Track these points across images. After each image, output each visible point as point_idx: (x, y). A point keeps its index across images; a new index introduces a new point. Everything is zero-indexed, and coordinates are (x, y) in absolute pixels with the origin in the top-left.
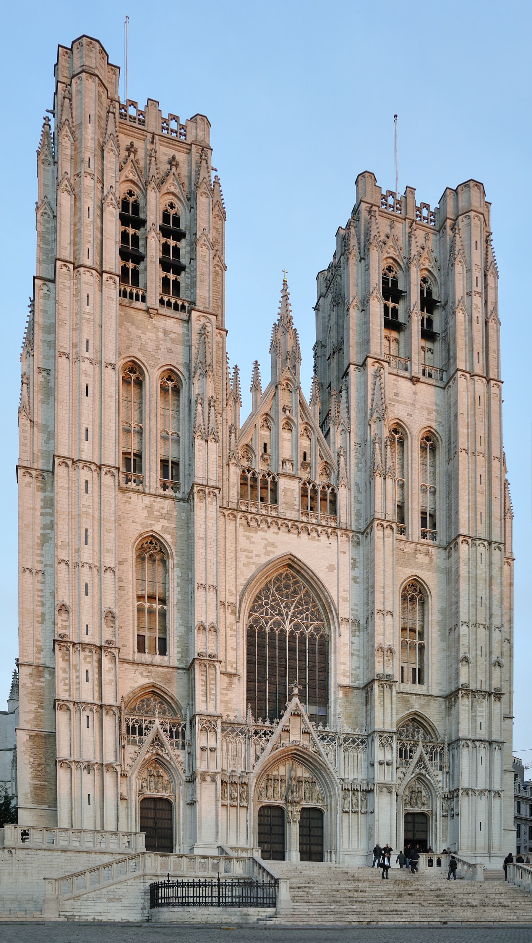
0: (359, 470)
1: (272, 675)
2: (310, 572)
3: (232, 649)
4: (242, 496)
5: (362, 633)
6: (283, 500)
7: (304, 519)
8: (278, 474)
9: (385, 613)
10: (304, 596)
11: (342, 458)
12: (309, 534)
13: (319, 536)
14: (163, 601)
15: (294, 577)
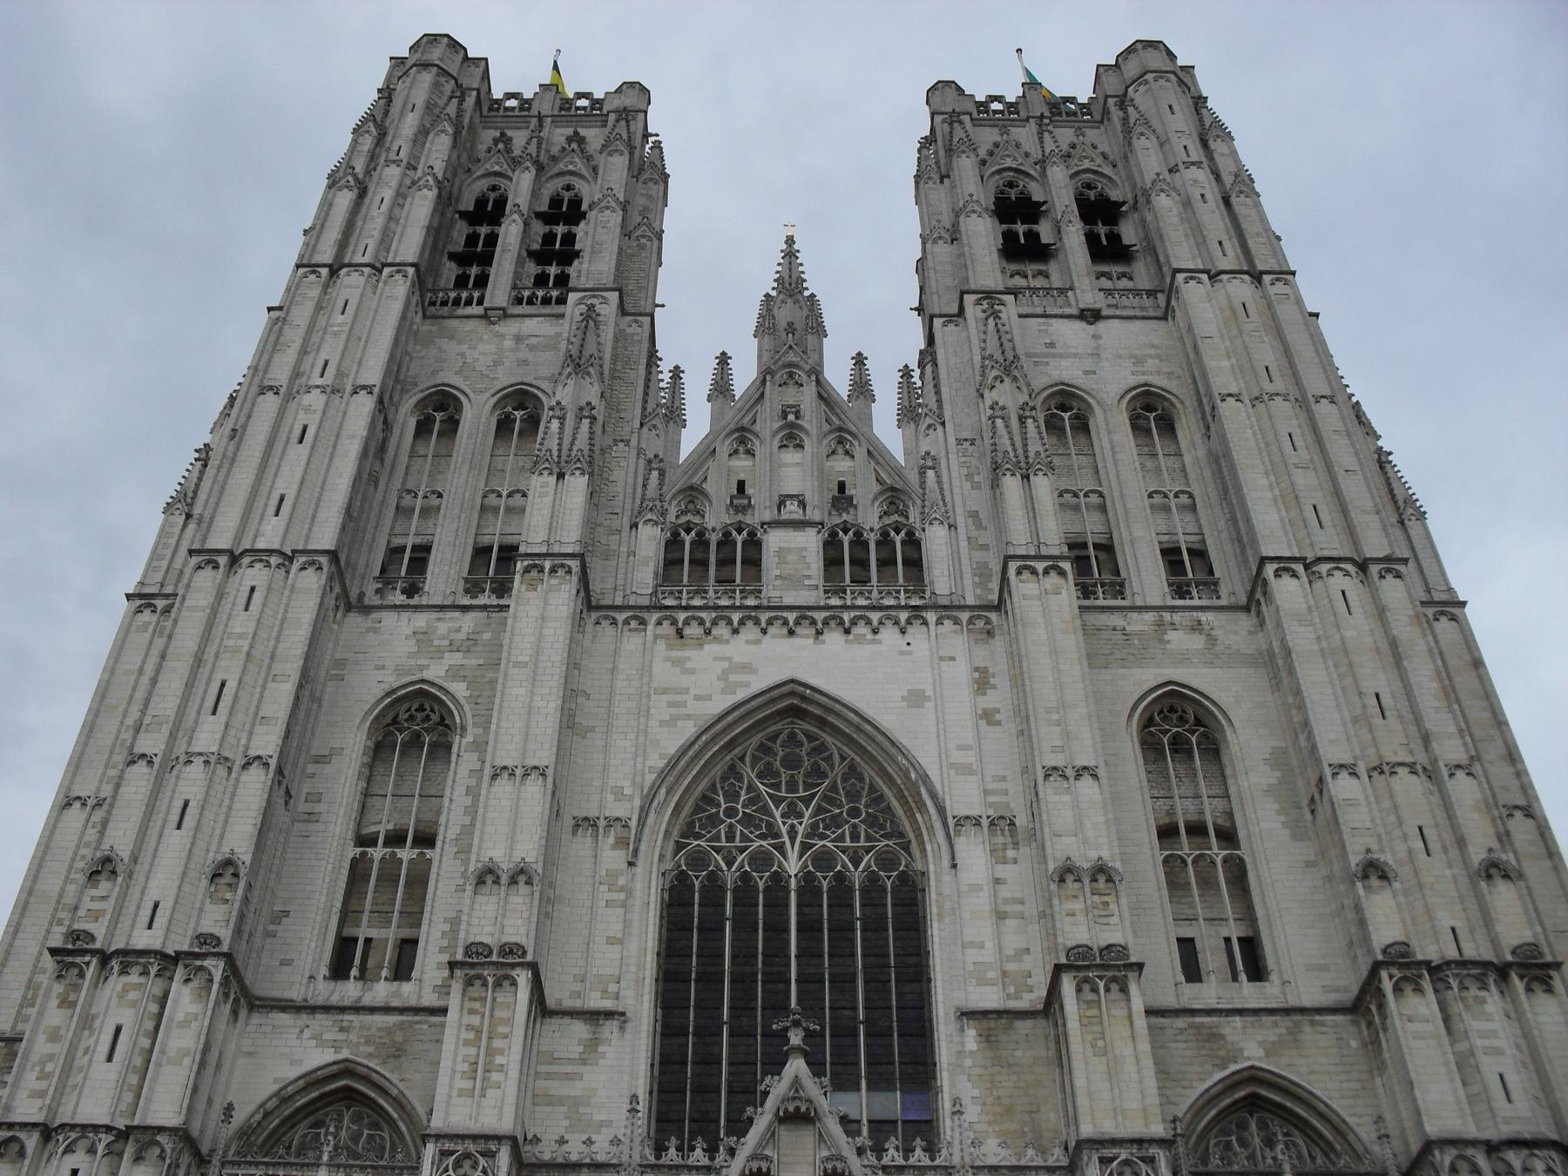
0: (976, 486)
1: (742, 1006)
2: (851, 715)
3: (611, 941)
5: (1024, 851)
6: (778, 572)
7: (835, 601)
8: (763, 524)
9: (1070, 773)
10: (845, 779)
11: (930, 474)
12: (847, 632)
13: (875, 632)
14: (426, 840)
15: (811, 737)
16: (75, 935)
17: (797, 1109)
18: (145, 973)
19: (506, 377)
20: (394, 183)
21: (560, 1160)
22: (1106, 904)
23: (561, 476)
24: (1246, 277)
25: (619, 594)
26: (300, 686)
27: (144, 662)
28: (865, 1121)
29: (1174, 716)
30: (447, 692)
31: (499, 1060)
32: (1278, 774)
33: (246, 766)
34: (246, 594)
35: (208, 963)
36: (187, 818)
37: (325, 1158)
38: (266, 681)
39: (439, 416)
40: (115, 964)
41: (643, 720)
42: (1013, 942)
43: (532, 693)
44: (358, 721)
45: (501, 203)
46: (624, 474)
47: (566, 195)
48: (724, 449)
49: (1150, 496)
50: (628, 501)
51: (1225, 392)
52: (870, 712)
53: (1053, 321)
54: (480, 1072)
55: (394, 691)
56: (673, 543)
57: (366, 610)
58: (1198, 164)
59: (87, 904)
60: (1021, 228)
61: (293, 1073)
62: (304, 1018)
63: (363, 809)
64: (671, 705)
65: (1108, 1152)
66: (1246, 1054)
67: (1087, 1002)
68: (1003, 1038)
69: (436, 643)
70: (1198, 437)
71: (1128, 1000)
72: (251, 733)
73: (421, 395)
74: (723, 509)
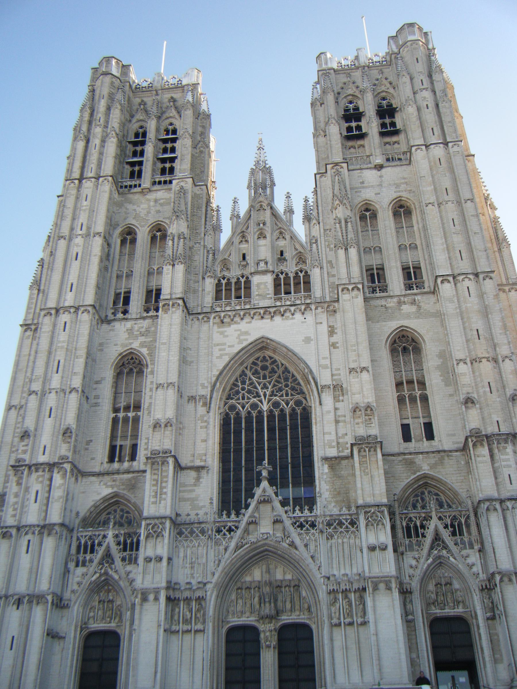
0: (331, 250)
1: (249, 460)
4: (218, 297)
6: (257, 293)
7: (278, 304)
8: (251, 274)
9: (359, 370)
10: (283, 373)
11: (314, 245)
12: (283, 315)
15: (271, 358)
16: (18, 460)
17: (264, 499)
18: (44, 471)
19: (152, 219)
20: (99, 136)
21: (188, 522)
22: (370, 419)
23: (173, 265)
24: (441, 145)
25: (200, 307)
26: (87, 358)
27: (30, 351)
28: (291, 499)
29: (404, 339)
30: (140, 353)
31: (165, 490)
32: (441, 360)
33: (70, 392)
34: (63, 325)
35: (65, 465)
36: (52, 413)
37: (111, 527)
38: (74, 358)
39: (129, 237)
40: (33, 468)
41: (210, 357)
42: (341, 432)
43: (169, 355)
44: (110, 366)
45: (144, 135)
46: (199, 258)
47: (170, 128)
48: (237, 240)
49: (400, 246)
50: (201, 268)
51: (428, 202)
52: (291, 347)
53: (364, 171)
54: (159, 495)
55: (122, 353)
56: (218, 285)
57: (109, 322)
58: (426, 89)
59: (22, 448)
60: (354, 124)
61: (98, 497)
62: (101, 478)
63: (115, 398)
64: (220, 350)
65: (368, 510)
66: (423, 468)
67: (363, 456)
68: (337, 467)
69: (135, 333)
70: (419, 219)
71: (377, 454)
72: (71, 379)
73: (121, 230)
74: (237, 267)
